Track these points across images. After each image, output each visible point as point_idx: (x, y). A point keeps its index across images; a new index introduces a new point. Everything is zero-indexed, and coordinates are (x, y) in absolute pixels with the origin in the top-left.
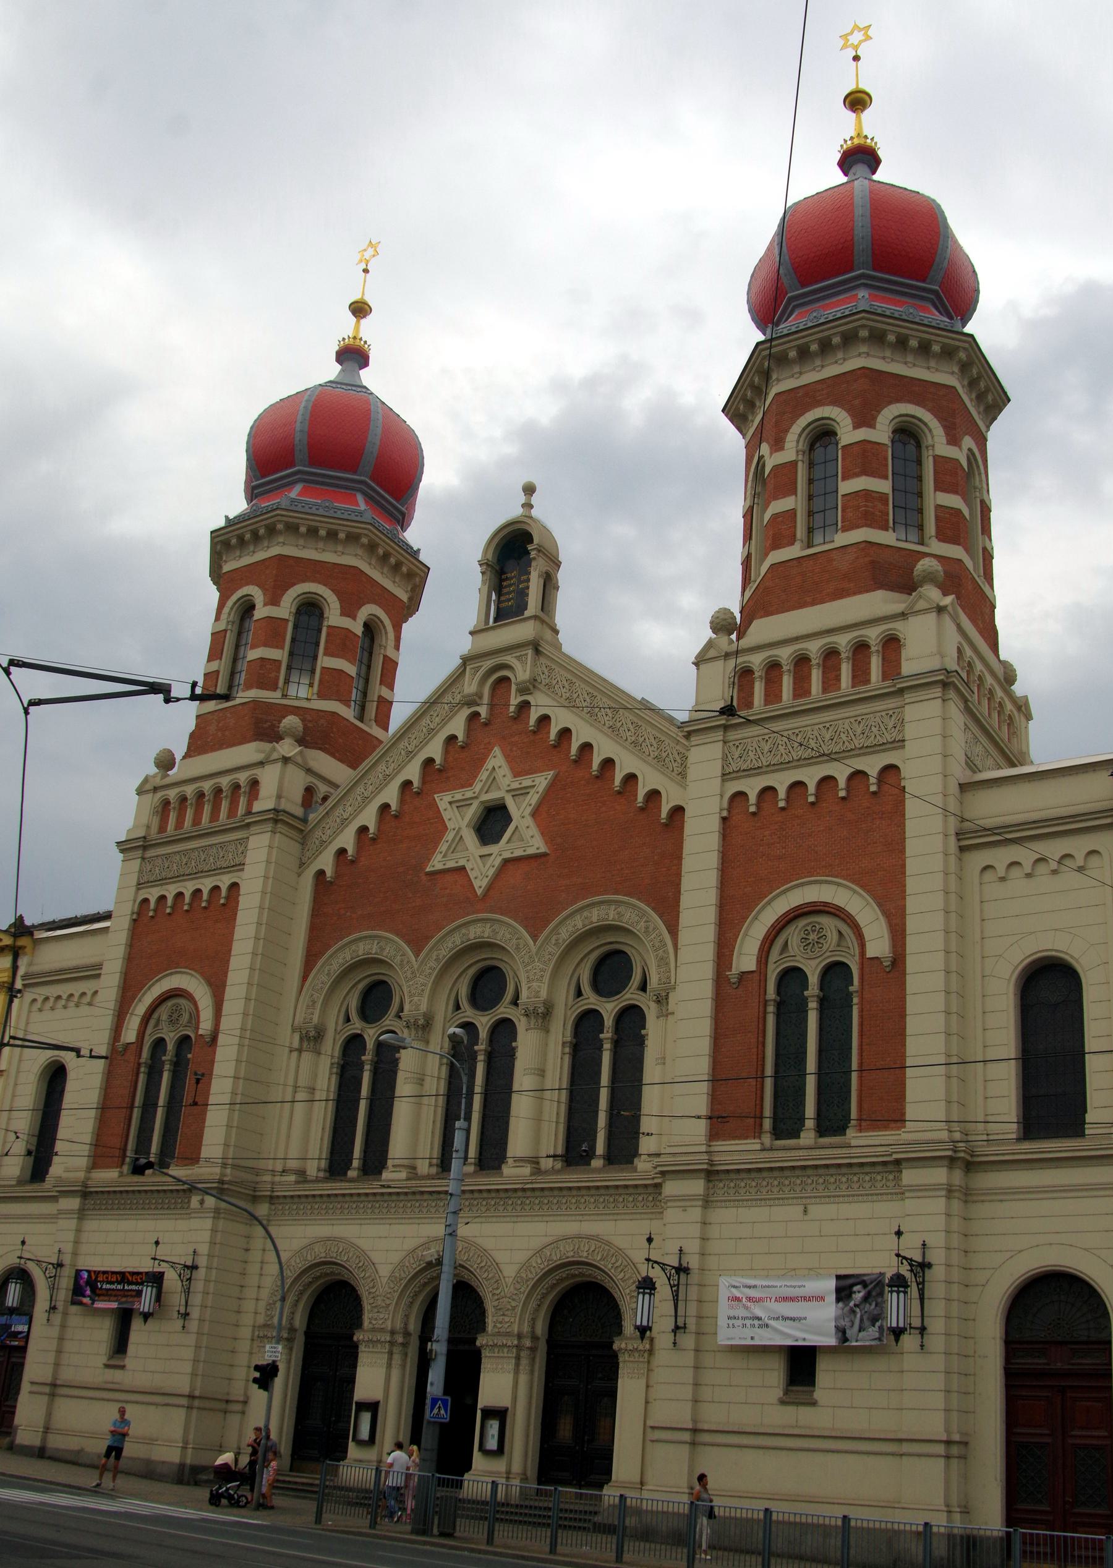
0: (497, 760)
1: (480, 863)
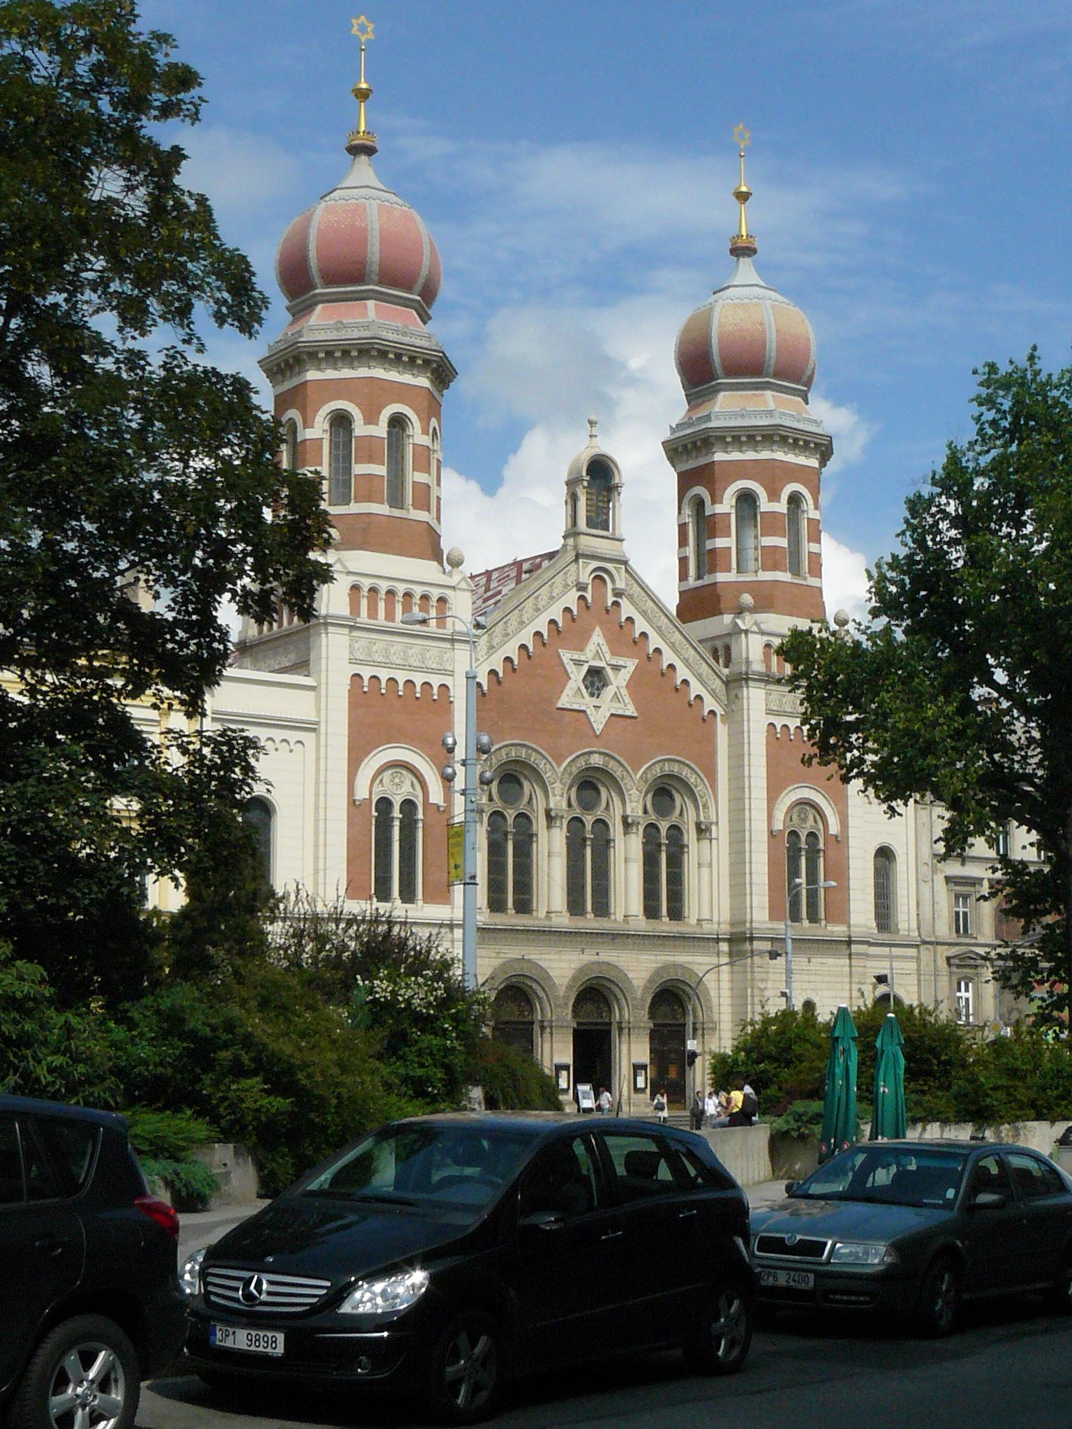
0: (597, 637)
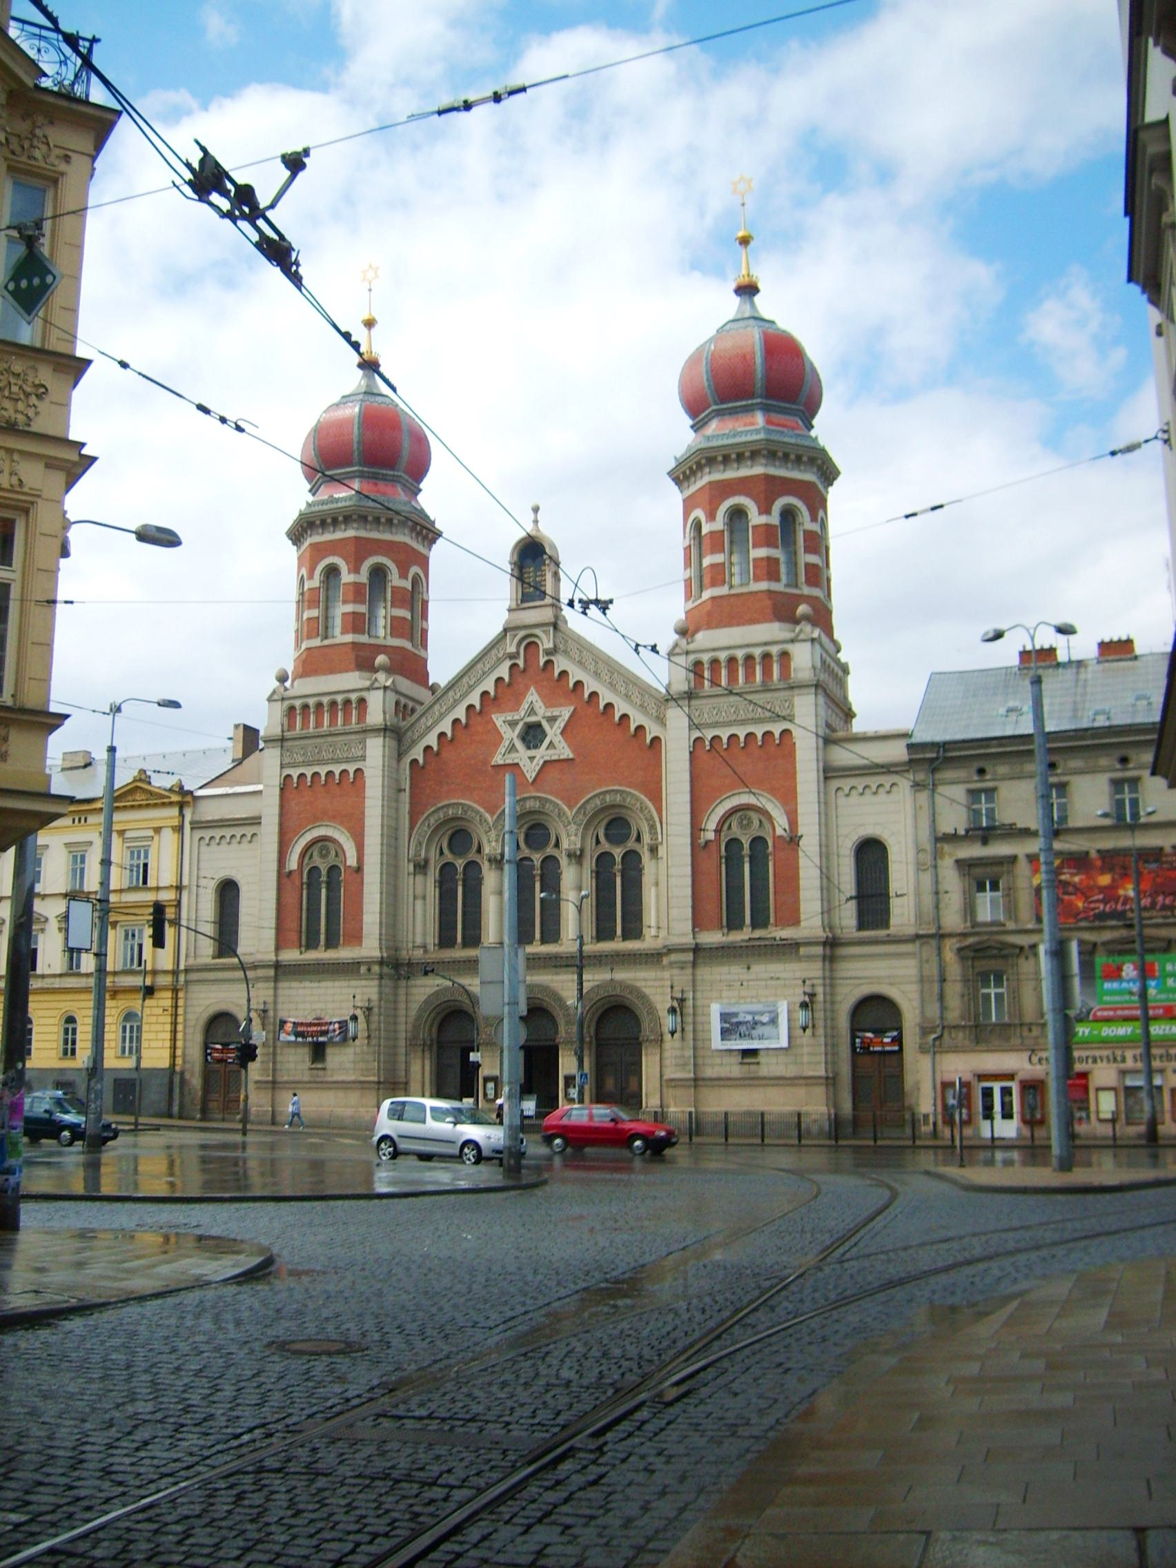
0: (533, 696)
1: (530, 762)
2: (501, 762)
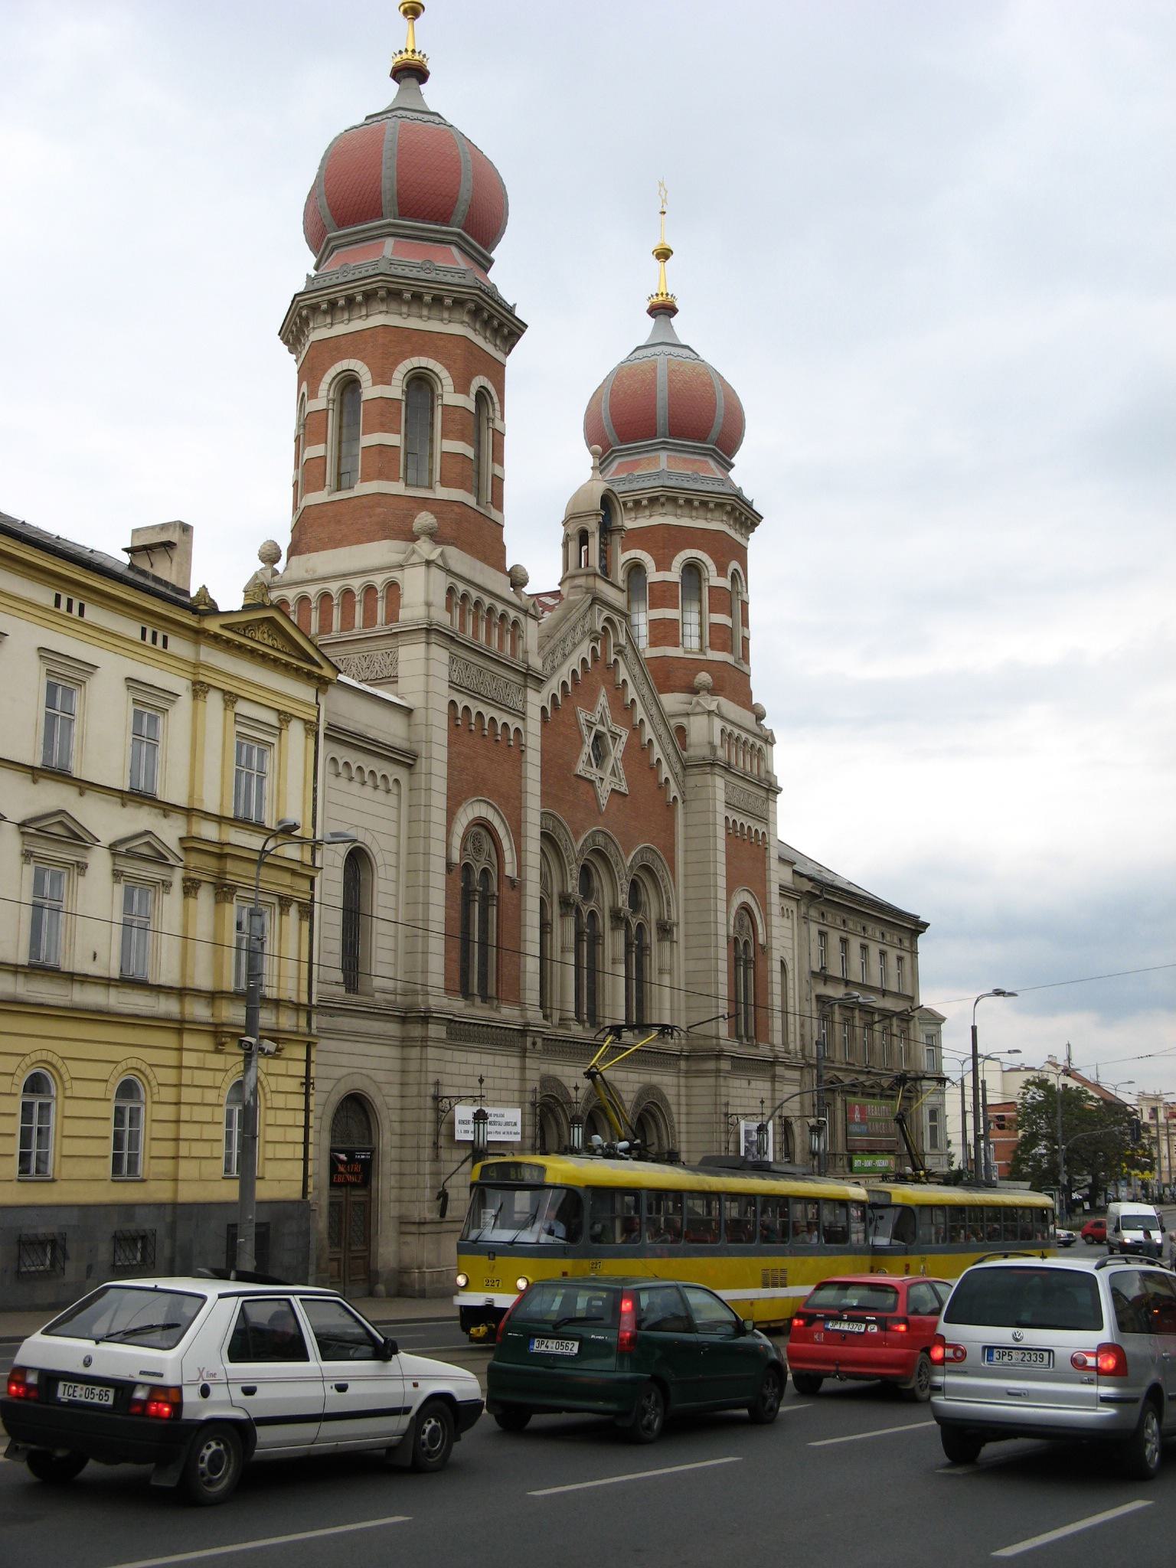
2: (582, 774)
